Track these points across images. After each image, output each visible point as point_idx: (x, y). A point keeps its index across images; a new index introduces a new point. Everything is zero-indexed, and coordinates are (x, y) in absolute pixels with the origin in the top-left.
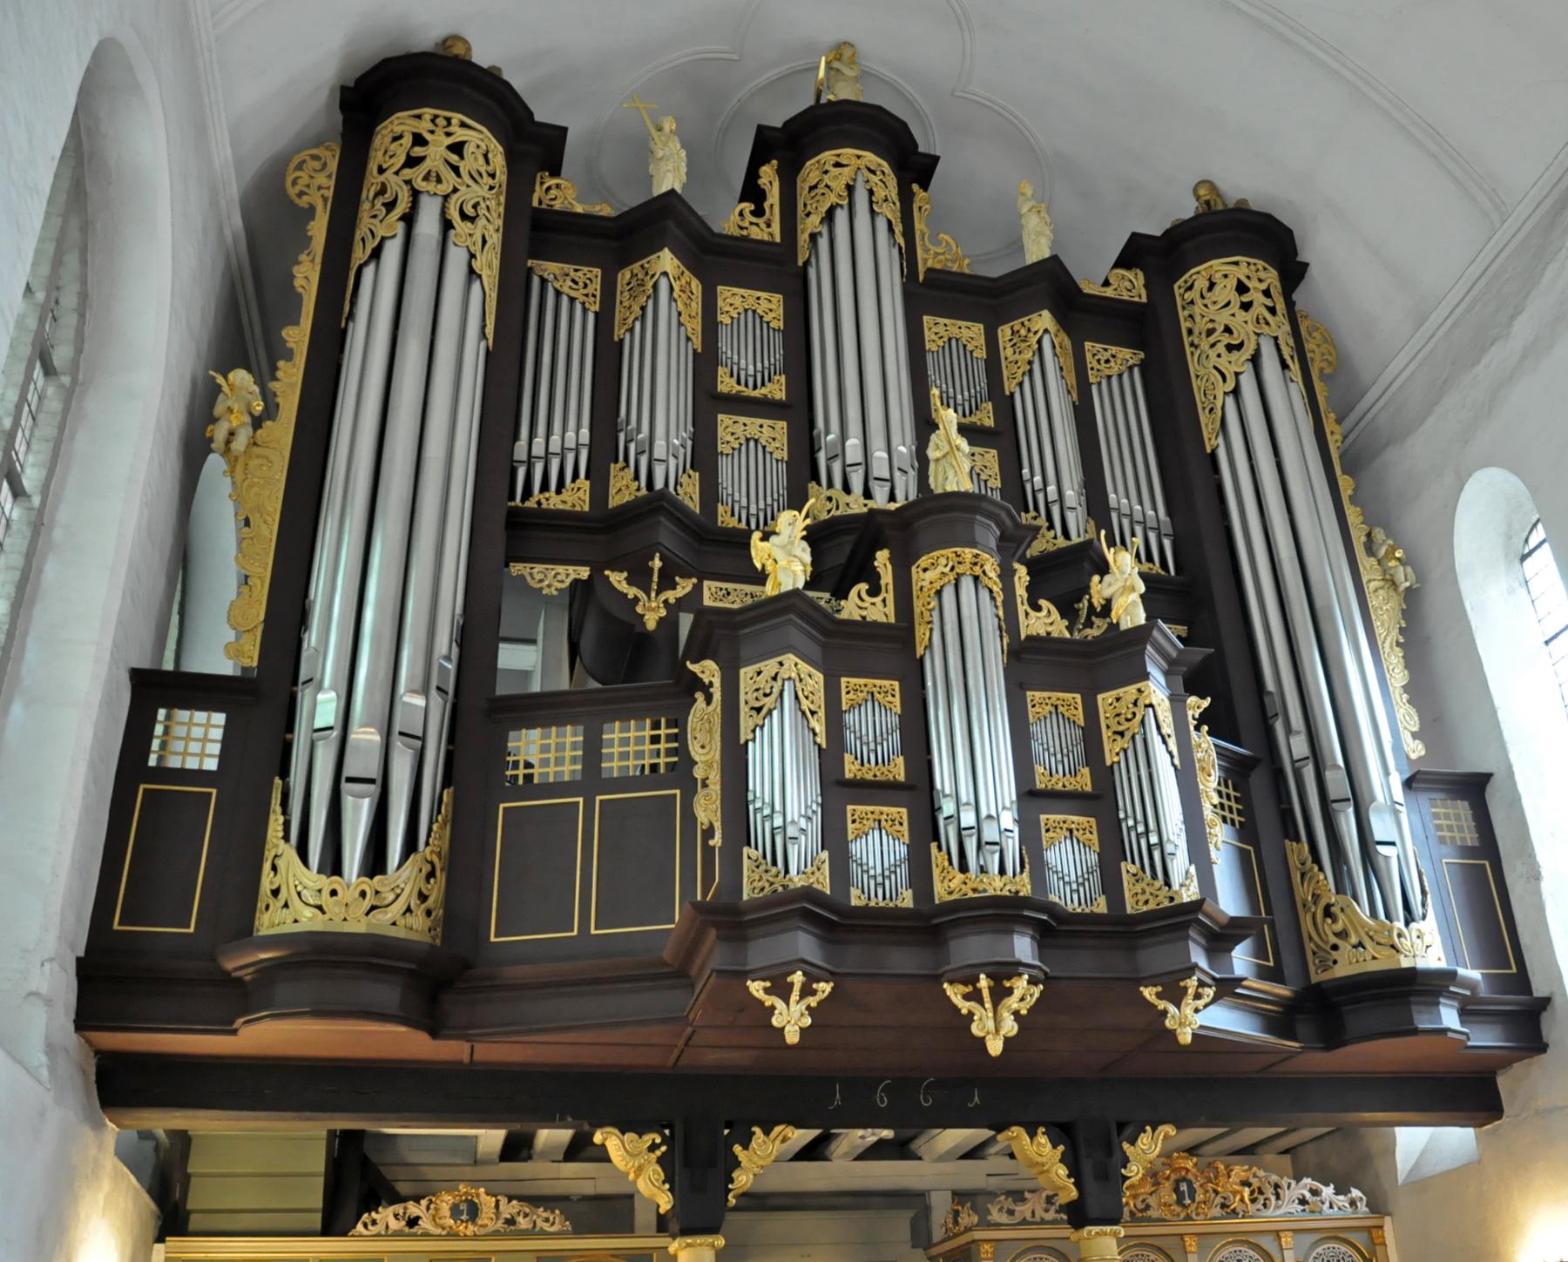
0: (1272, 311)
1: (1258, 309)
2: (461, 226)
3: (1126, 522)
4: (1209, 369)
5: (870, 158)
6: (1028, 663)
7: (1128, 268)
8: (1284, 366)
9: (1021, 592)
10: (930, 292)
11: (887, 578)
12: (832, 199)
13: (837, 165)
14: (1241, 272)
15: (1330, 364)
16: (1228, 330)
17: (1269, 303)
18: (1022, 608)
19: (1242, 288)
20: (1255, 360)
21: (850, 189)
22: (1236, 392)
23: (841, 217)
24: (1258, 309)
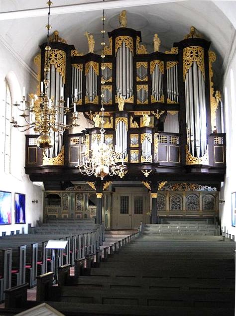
0: (197, 56)
1: (194, 56)
2: (58, 68)
3: (172, 95)
4: (186, 67)
5: (126, 37)
6: (131, 131)
7: (175, 47)
8: (198, 67)
9: (131, 120)
10: (137, 58)
11: (112, 121)
12: (119, 46)
13: (120, 39)
14: (191, 50)
15: (213, 60)
16: (188, 61)
17: (197, 55)
18: (131, 123)
19: (192, 53)
20: (192, 66)
21: (122, 44)
22: (188, 72)
23: (121, 49)
24: (194, 56)
